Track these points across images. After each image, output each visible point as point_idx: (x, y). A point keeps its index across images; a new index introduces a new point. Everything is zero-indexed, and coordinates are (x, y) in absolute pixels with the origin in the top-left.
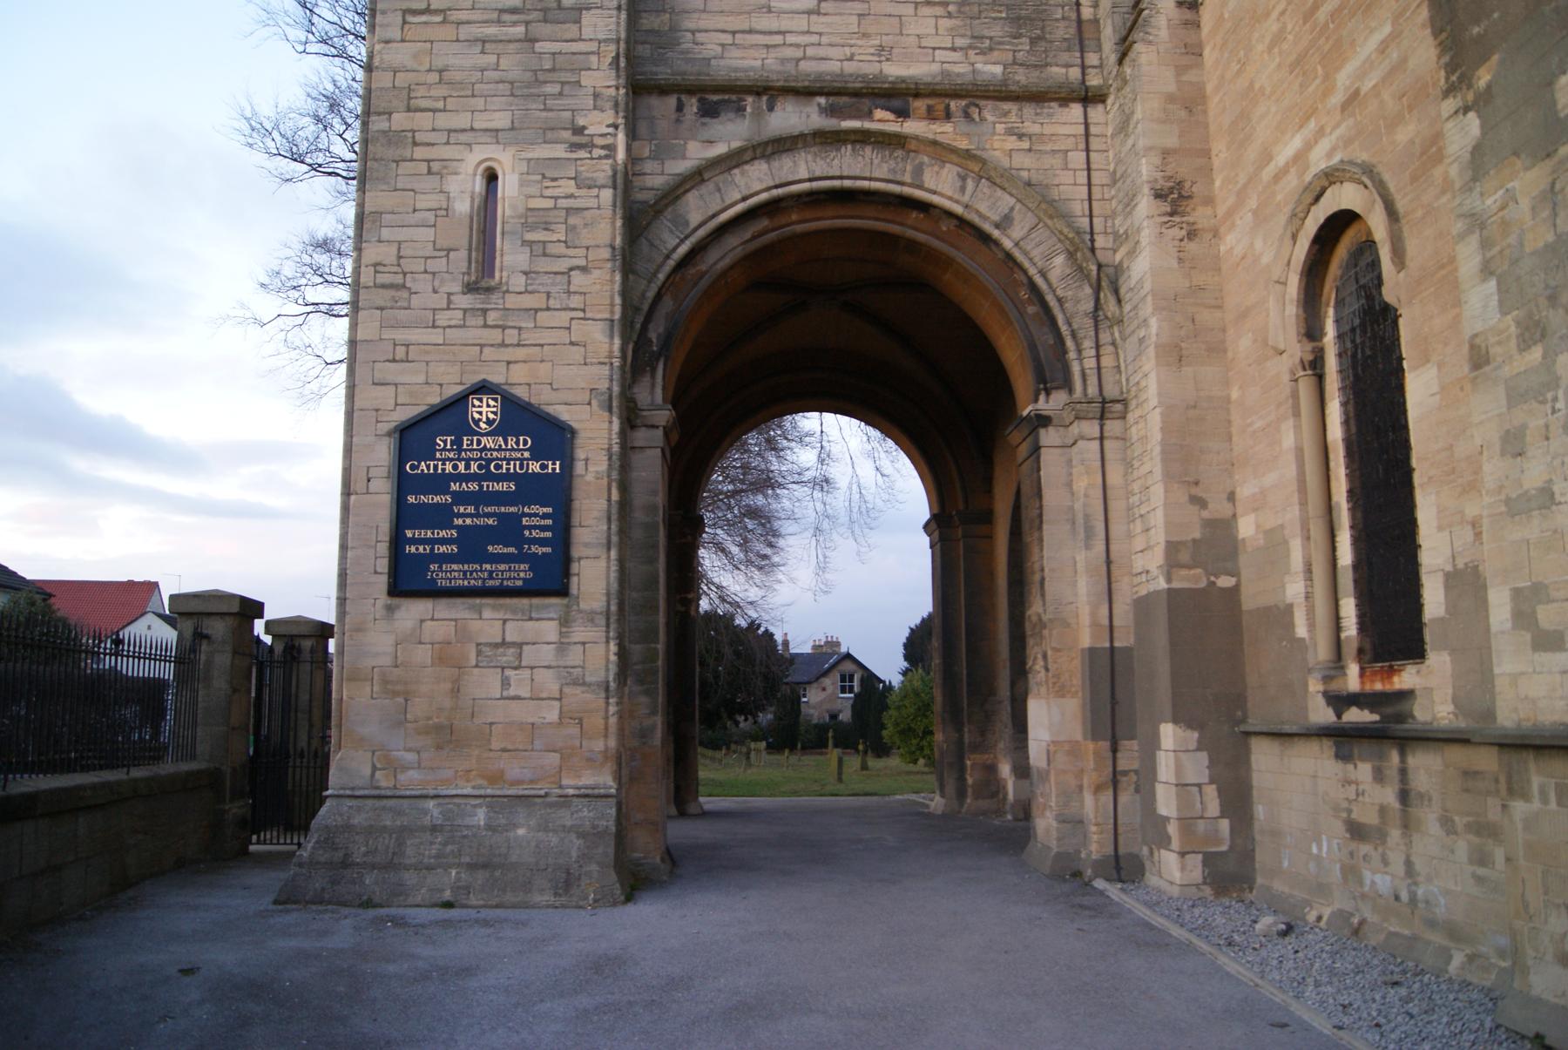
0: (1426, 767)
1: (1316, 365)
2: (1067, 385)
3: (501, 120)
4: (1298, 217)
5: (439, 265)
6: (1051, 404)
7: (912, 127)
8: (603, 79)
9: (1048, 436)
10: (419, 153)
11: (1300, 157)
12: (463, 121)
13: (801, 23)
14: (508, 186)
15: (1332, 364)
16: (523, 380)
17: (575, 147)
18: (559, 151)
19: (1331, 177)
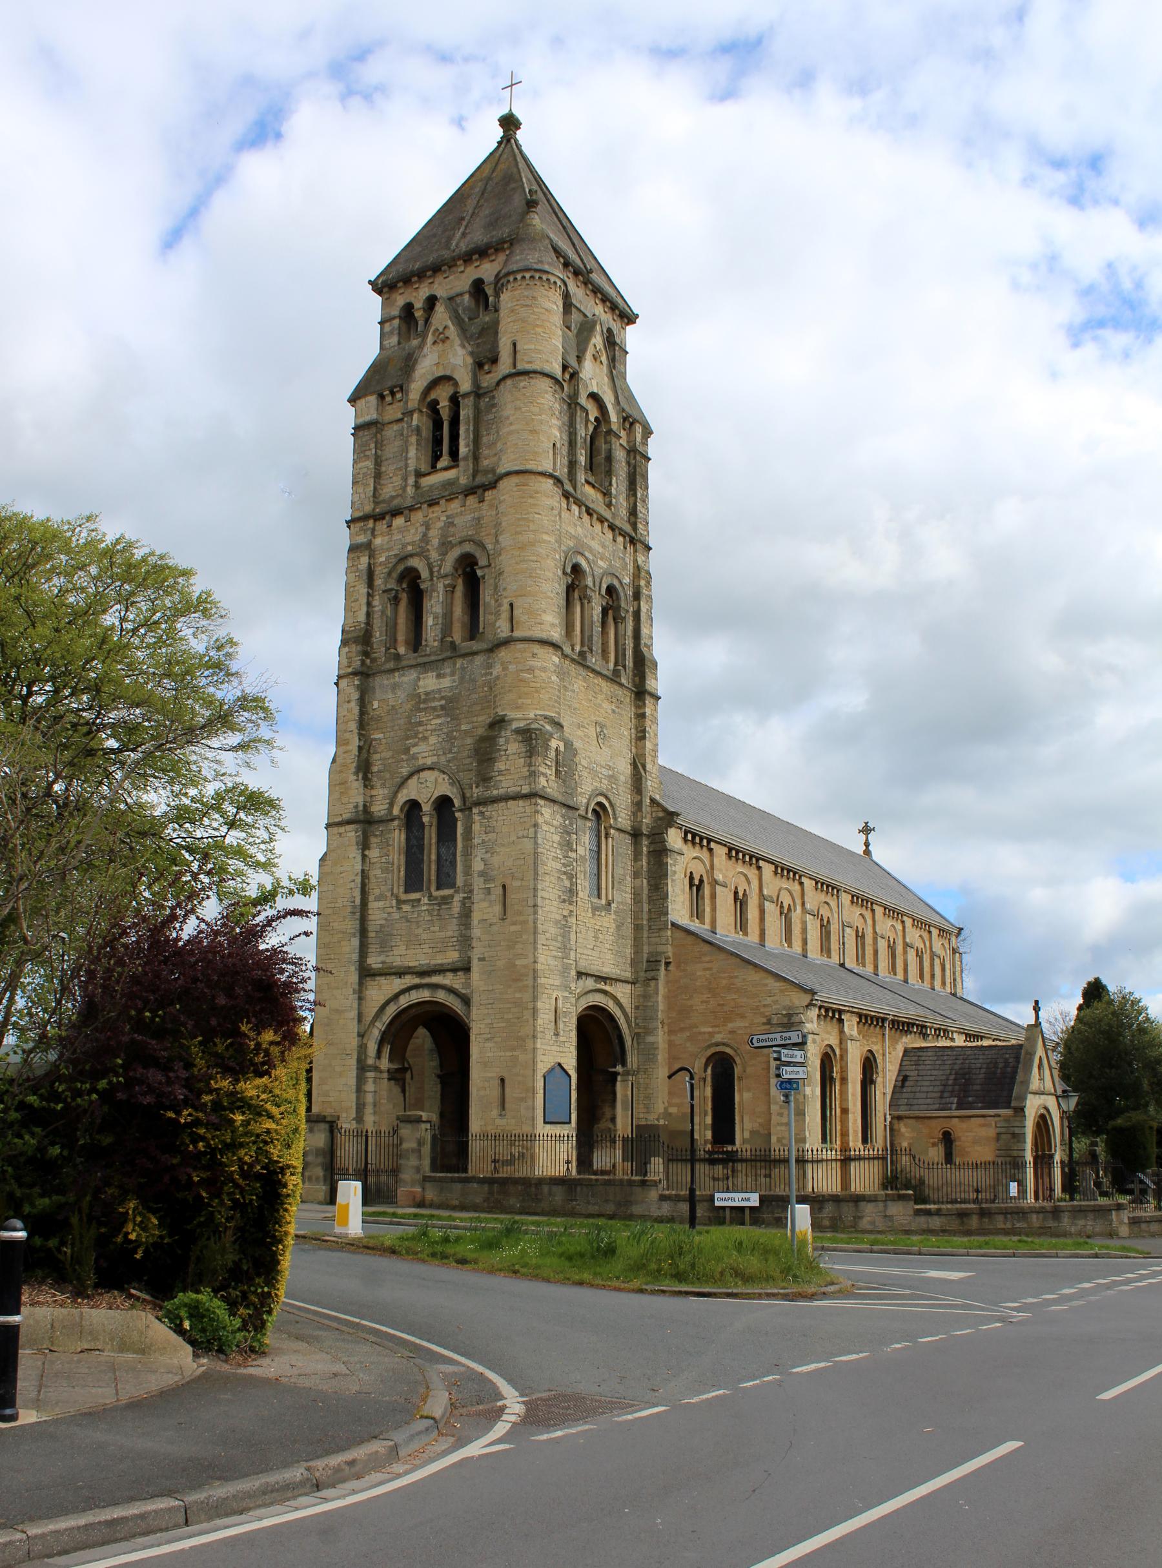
0: (739, 1166)
1: (705, 1080)
2: (624, 1064)
3: (557, 983)
4: (709, 1046)
5: (549, 1026)
6: (619, 1068)
7: (607, 988)
8: (573, 973)
9: (619, 1078)
10: (546, 991)
11: (711, 1034)
12: (551, 982)
13: (590, 952)
14: (560, 1004)
15: (709, 1079)
16: (562, 1061)
17: (570, 993)
18: (566, 994)
19: (724, 1044)
